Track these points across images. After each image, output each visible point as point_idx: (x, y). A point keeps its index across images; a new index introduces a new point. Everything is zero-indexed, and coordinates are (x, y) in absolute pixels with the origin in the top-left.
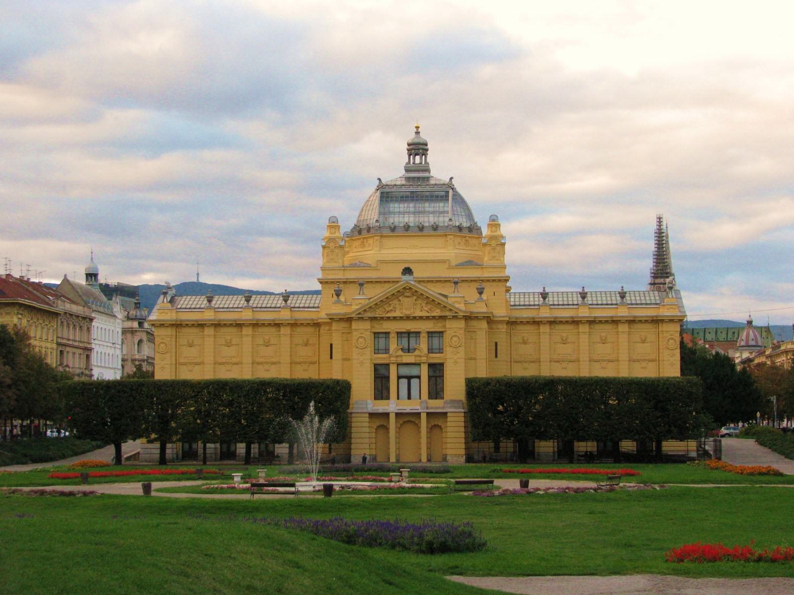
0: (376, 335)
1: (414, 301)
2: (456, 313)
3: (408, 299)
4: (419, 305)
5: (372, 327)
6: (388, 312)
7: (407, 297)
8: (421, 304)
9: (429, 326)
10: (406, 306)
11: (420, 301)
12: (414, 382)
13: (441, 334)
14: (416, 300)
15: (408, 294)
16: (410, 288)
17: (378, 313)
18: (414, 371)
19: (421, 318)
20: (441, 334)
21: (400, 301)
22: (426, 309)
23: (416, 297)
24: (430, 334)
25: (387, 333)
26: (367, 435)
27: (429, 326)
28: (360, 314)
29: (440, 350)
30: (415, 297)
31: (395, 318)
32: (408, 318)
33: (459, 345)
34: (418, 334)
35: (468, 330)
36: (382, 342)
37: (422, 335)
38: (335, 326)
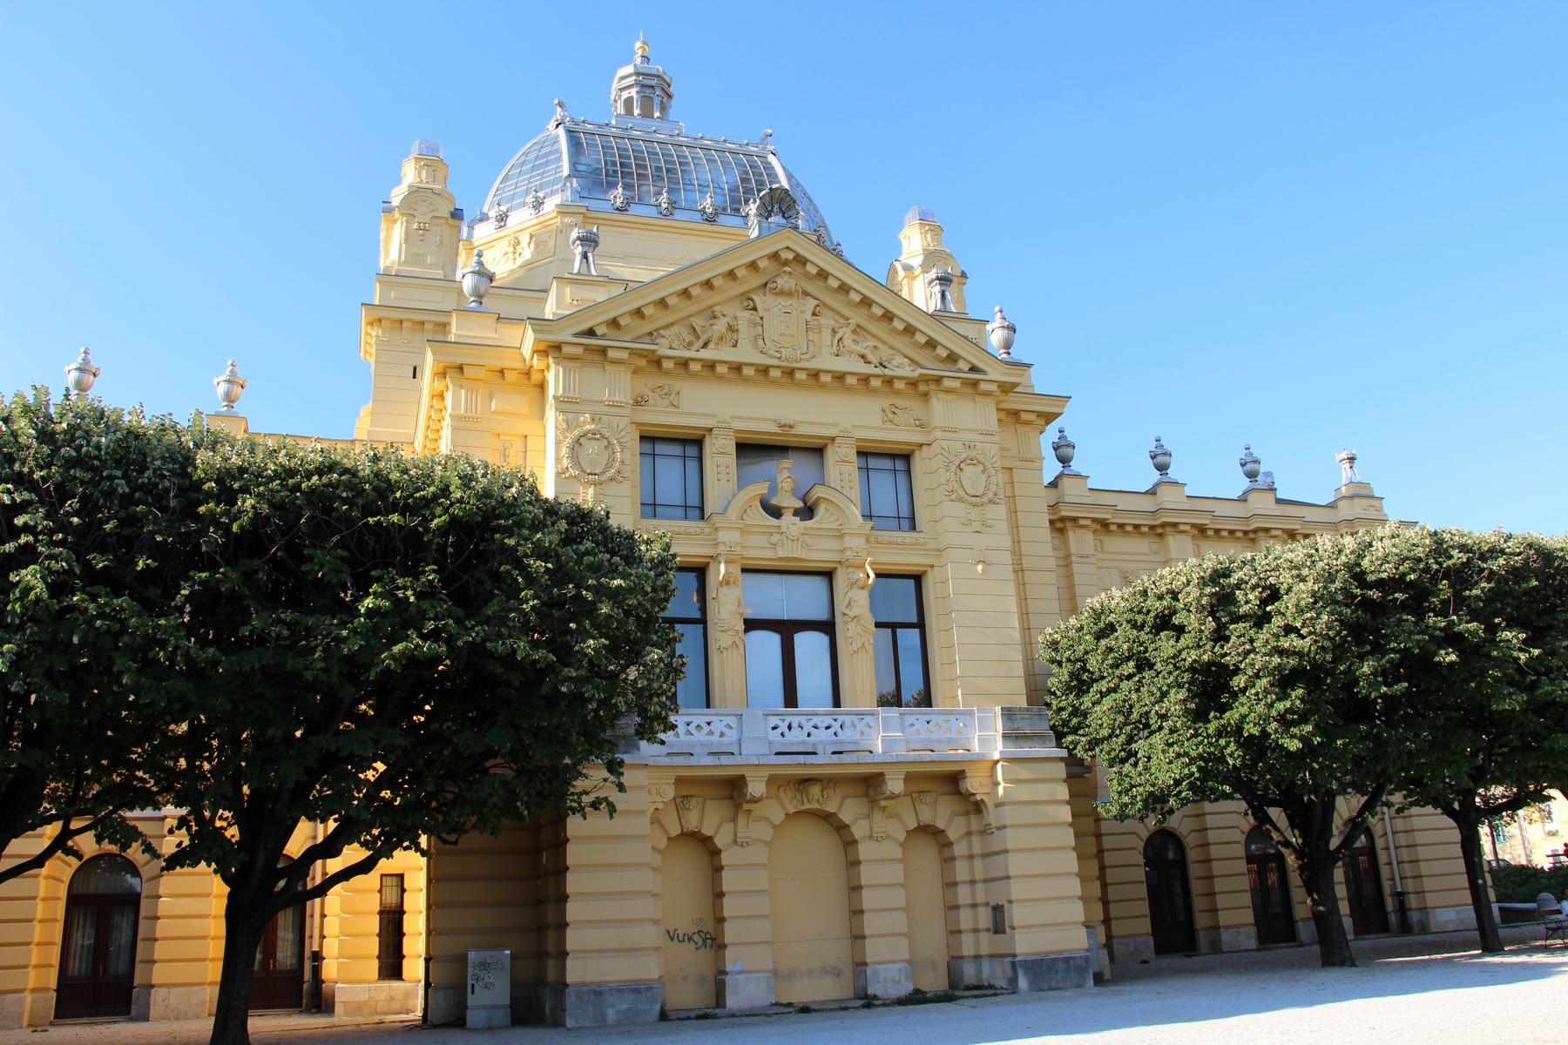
1: (808, 316)
2: (973, 369)
3: (785, 302)
4: (827, 333)
5: (639, 402)
6: (705, 345)
7: (782, 293)
8: (834, 332)
11: (827, 321)
12: (809, 646)
13: (903, 458)
14: (814, 314)
15: (784, 282)
16: (801, 260)
18: (803, 599)
20: (903, 458)
21: (755, 309)
22: (860, 349)
23: (813, 303)
25: (693, 443)
26: (647, 880)
28: (591, 333)
30: (813, 303)
33: (991, 495)
36: (671, 472)
37: (831, 455)
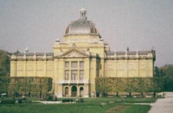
0: (66, 62)
9: (81, 60)
10: (74, 54)
13: (83, 62)
17: (66, 56)
19: (77, 58)
20: (83, 62)
24: (80, 62)
27: (81, 60)
29: (83, 67)
31: (70, 58)
32: (74, 58)
34: (77, 62)
35: (90, 60)
38: (55, 60)
